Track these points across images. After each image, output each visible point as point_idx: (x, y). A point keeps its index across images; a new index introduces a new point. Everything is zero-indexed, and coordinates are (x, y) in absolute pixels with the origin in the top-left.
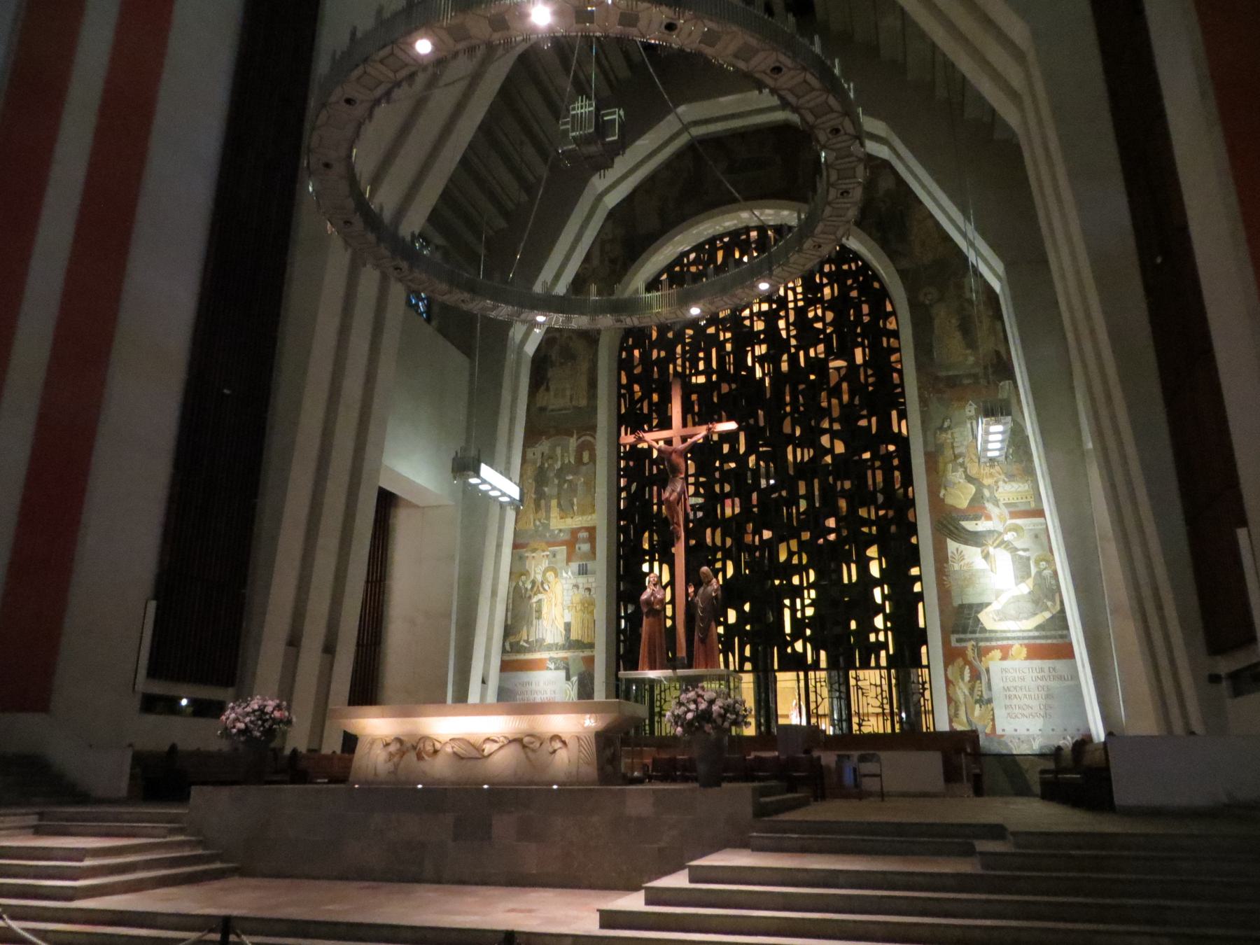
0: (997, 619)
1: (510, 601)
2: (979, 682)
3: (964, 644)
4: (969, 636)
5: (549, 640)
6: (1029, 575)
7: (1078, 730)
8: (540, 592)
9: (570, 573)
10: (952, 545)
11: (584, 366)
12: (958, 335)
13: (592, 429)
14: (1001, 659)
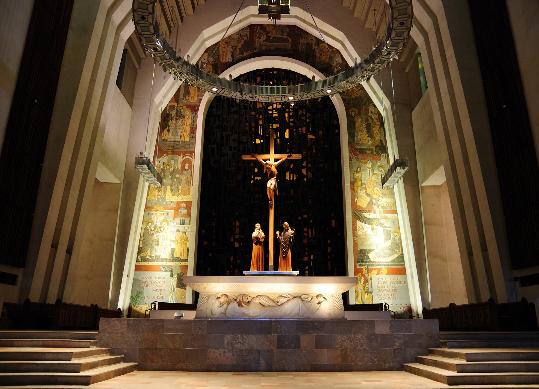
0: (376, 256)
1: (142, 235)
2: (367, 284)
3: (362, 267)
4: (364, 264)
5: (162, 256)
6: (390, 239)
7: (406, 305)
9: (175, 224)
10: (359, 223)
11: (189, 122)
12: (365, 131)
13: (192, 153)
14: (377, 274)
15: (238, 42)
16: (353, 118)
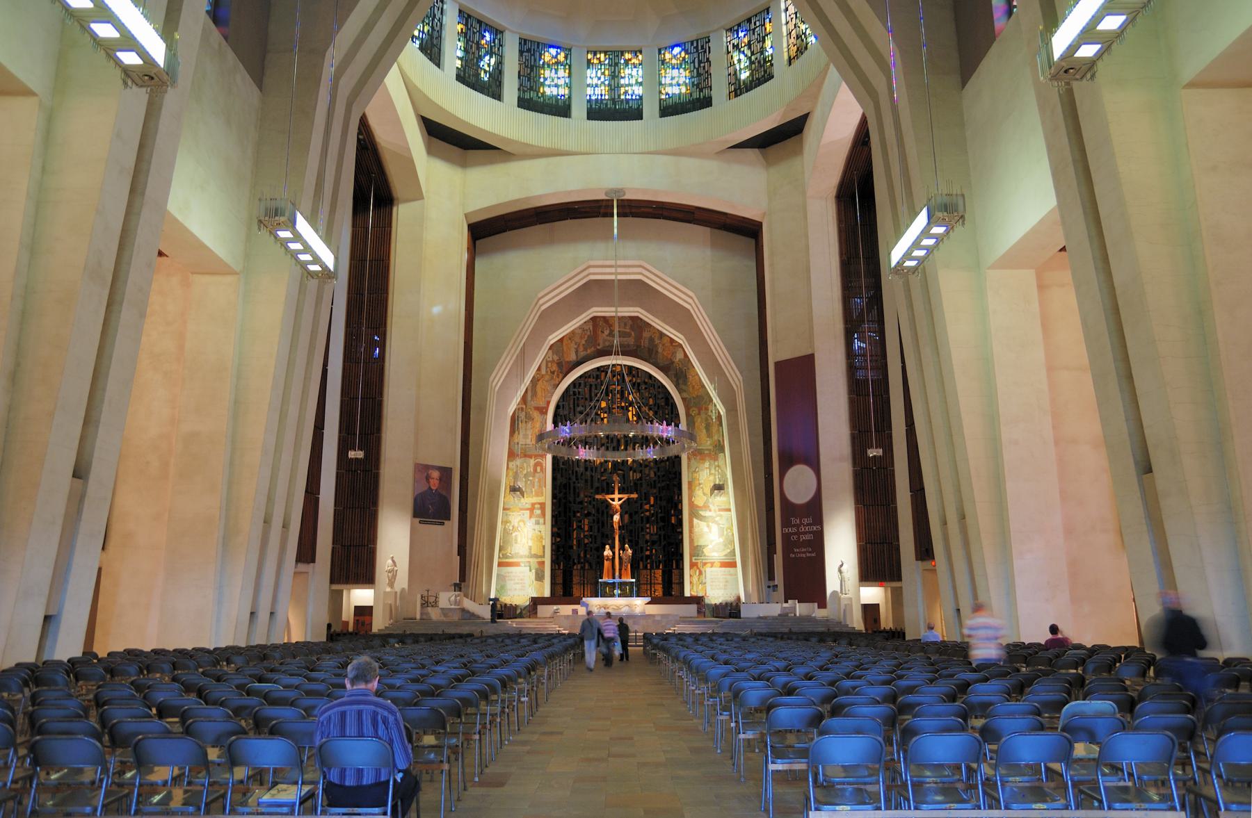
6: (723, 535)
10: (695, 521)
12: (704, 431)
15: (581, 338)
16: (693, 417)
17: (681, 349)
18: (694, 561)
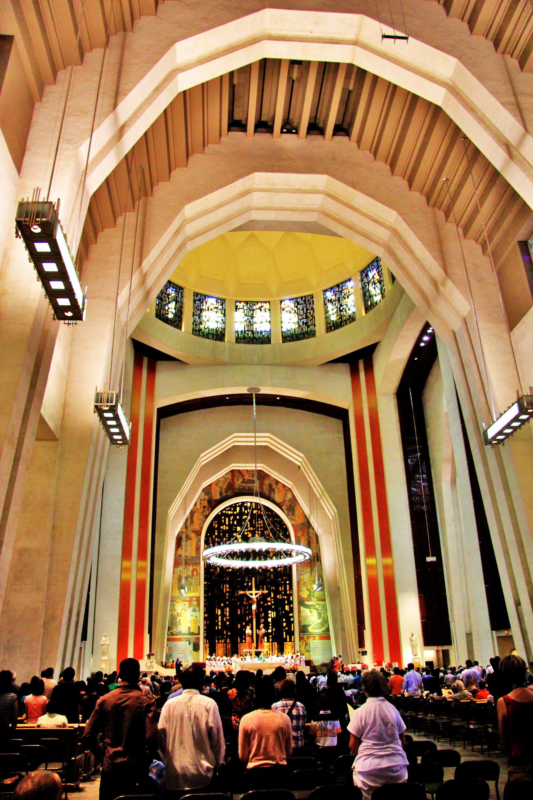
5: (183, 632)
8: (179, 616)
10: (302, 608)
11: (194, 543)
15: (224, 484)
16: (299, 538)
17: (290, 492)
18: (301, 636)
